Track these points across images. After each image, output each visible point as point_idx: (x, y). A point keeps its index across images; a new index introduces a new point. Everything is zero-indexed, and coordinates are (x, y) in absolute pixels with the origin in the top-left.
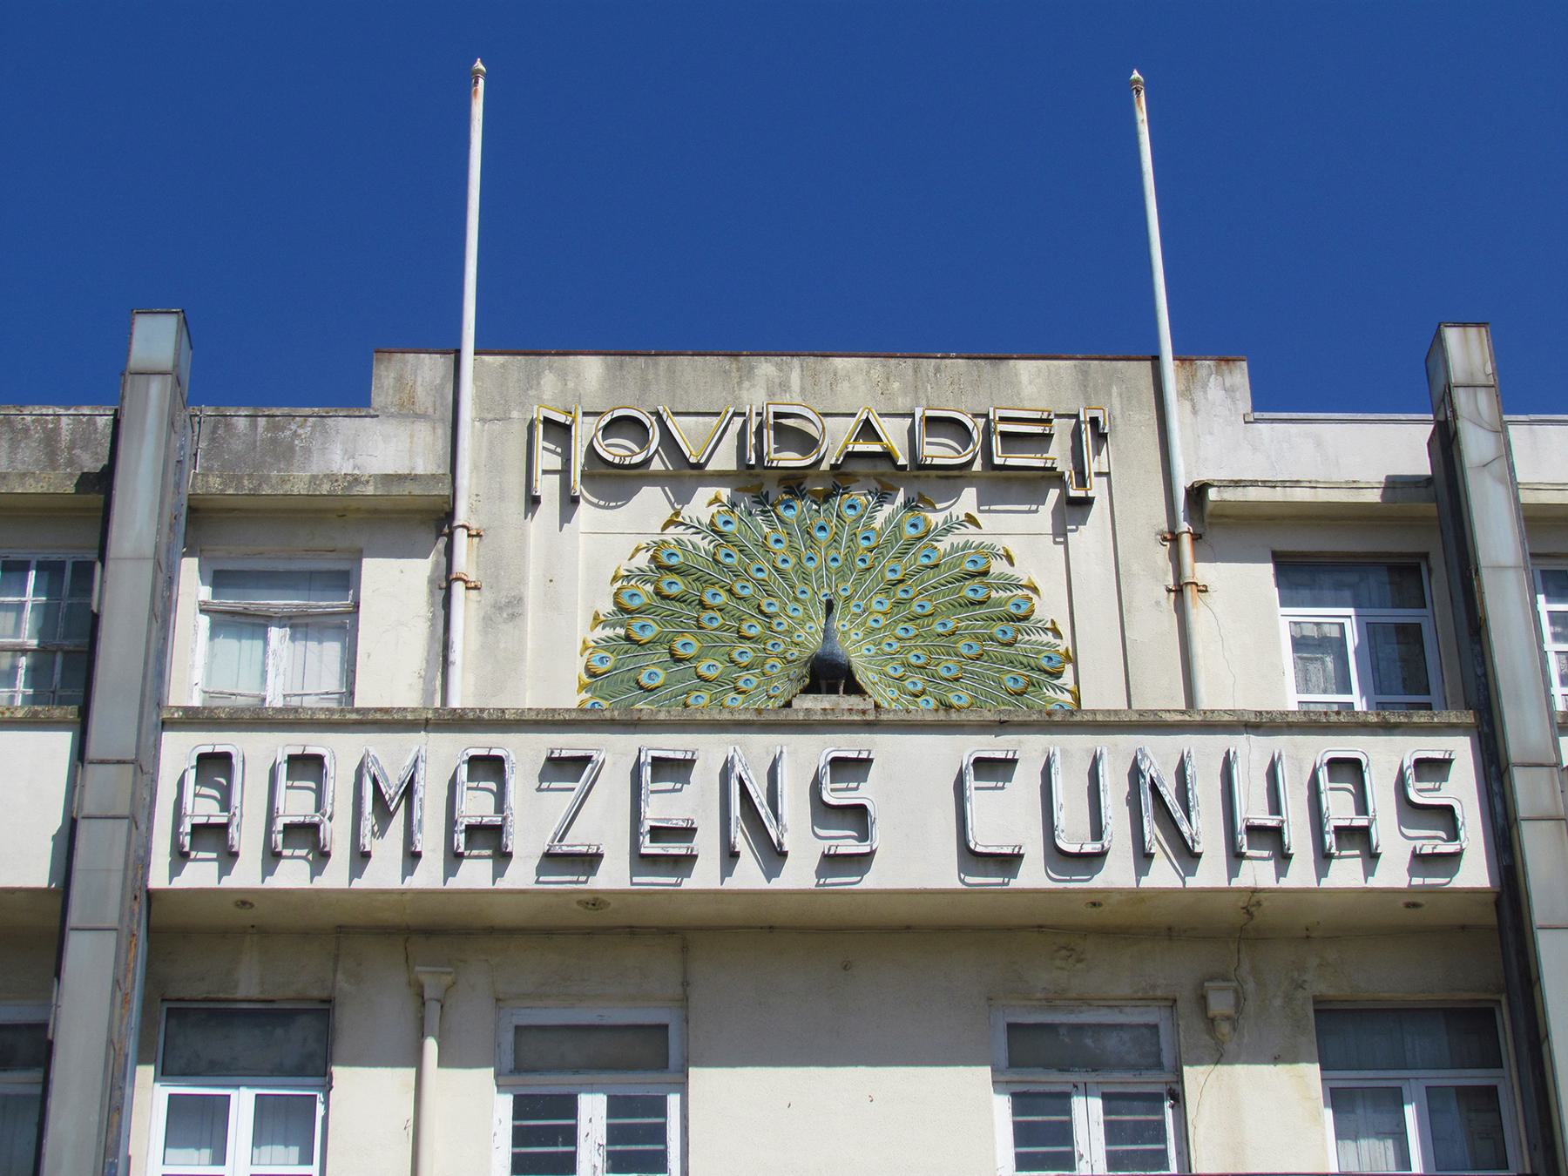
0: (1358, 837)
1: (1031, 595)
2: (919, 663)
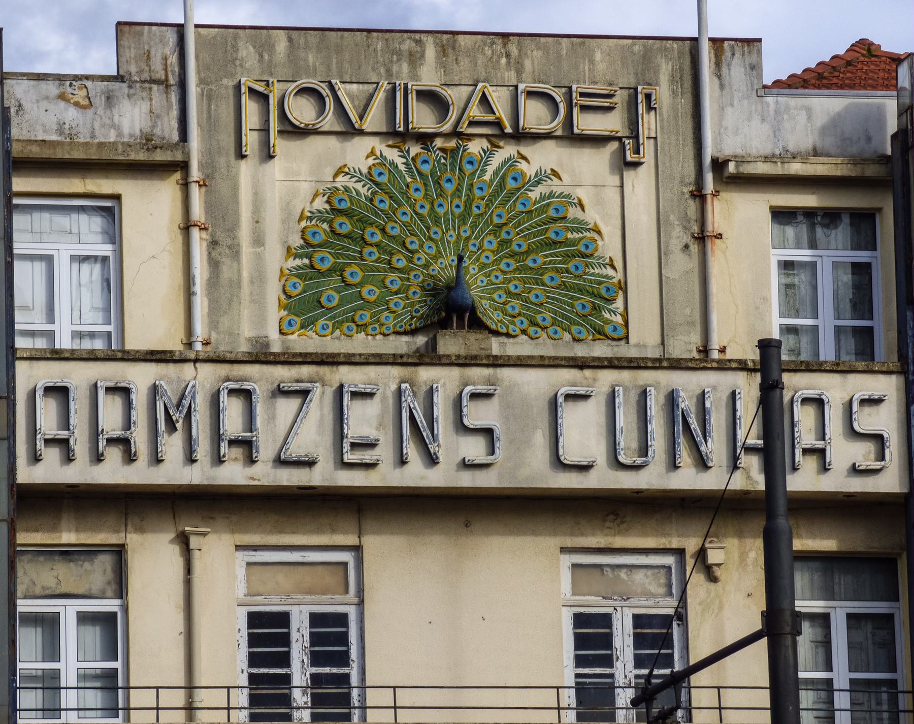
1: (596, 236)
2: (516, 291)
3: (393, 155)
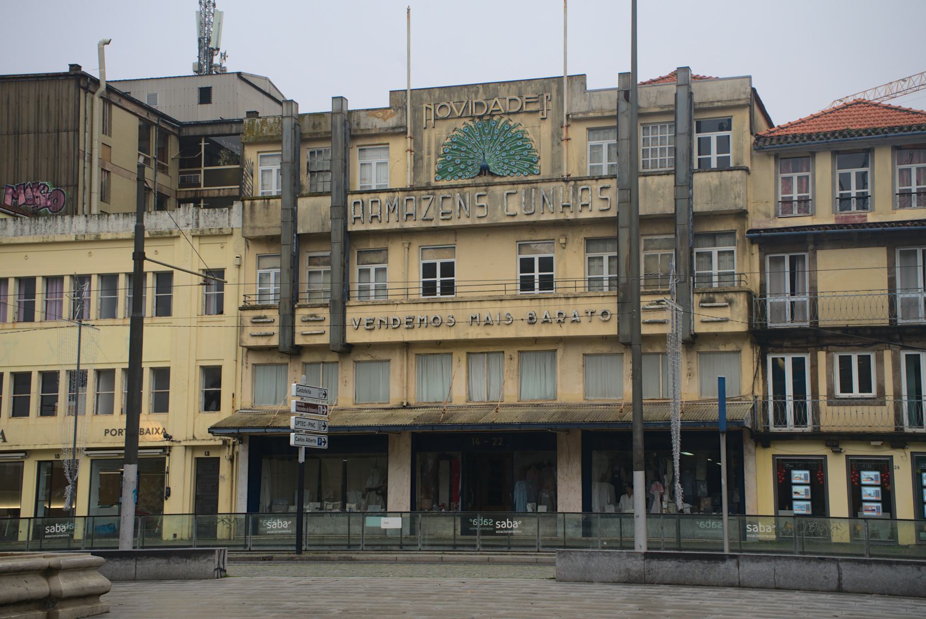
3: (471, 123)
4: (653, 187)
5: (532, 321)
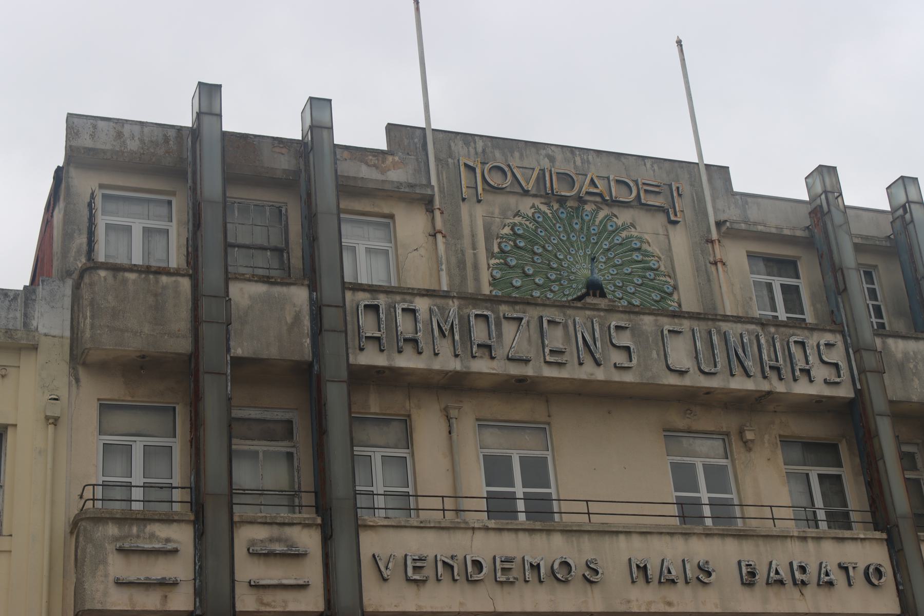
0: (807, 372)
3: (544, 208)
4: (899, 356)
5: (749, 579)
